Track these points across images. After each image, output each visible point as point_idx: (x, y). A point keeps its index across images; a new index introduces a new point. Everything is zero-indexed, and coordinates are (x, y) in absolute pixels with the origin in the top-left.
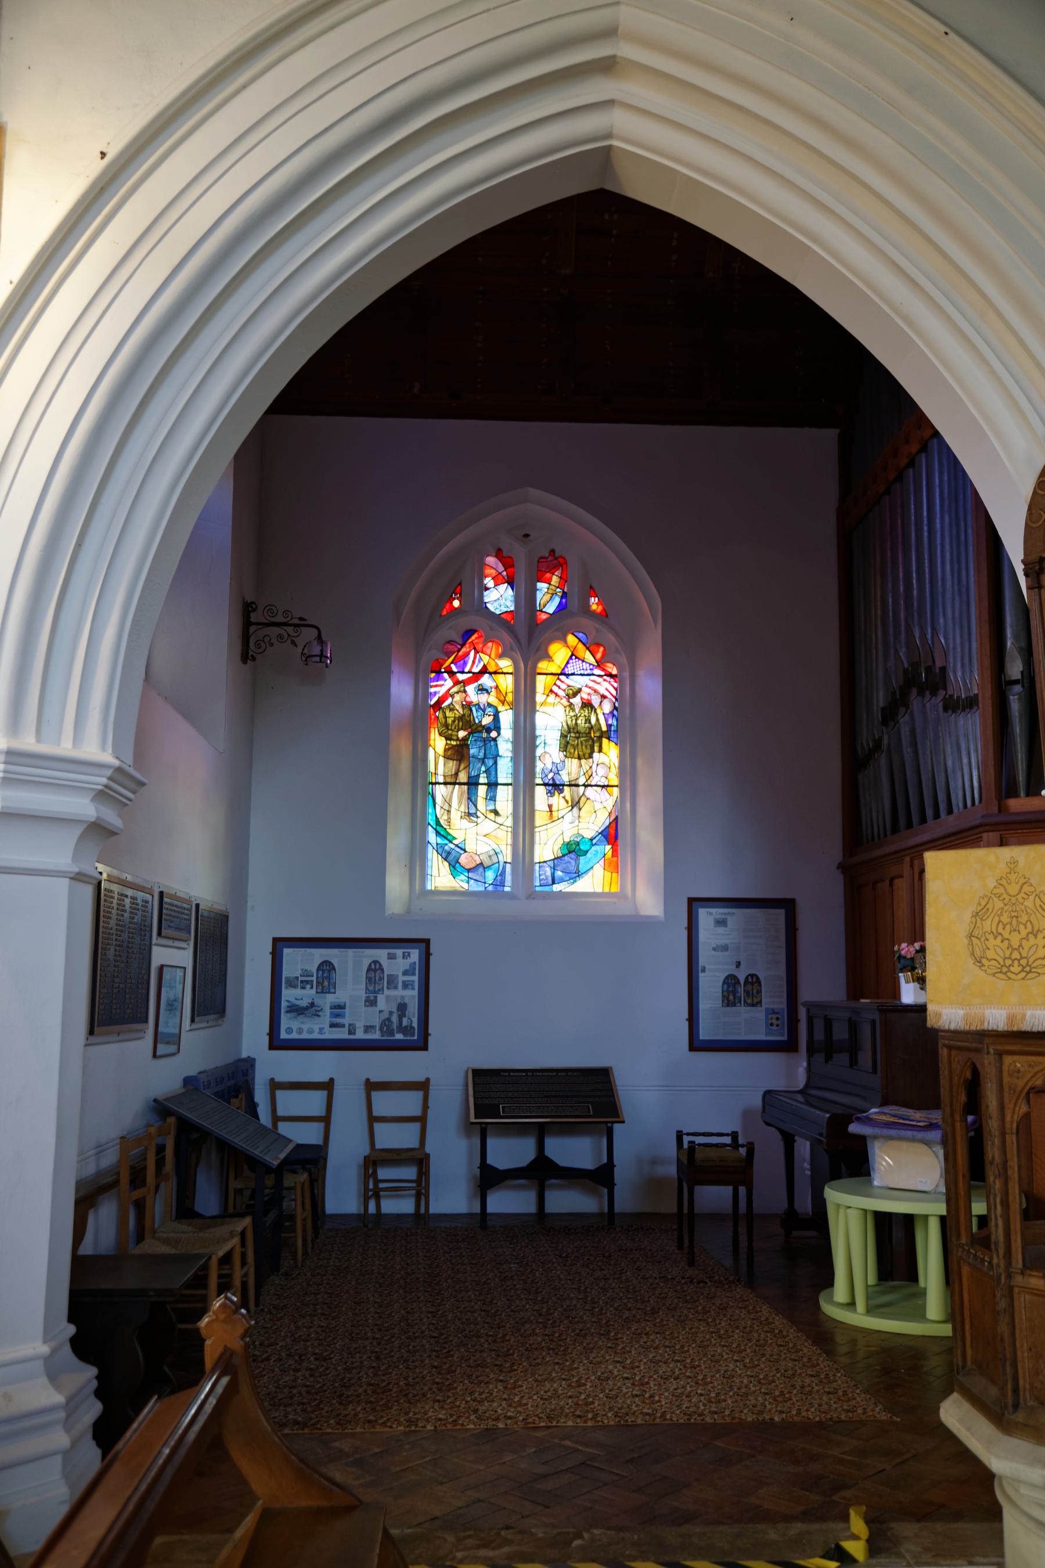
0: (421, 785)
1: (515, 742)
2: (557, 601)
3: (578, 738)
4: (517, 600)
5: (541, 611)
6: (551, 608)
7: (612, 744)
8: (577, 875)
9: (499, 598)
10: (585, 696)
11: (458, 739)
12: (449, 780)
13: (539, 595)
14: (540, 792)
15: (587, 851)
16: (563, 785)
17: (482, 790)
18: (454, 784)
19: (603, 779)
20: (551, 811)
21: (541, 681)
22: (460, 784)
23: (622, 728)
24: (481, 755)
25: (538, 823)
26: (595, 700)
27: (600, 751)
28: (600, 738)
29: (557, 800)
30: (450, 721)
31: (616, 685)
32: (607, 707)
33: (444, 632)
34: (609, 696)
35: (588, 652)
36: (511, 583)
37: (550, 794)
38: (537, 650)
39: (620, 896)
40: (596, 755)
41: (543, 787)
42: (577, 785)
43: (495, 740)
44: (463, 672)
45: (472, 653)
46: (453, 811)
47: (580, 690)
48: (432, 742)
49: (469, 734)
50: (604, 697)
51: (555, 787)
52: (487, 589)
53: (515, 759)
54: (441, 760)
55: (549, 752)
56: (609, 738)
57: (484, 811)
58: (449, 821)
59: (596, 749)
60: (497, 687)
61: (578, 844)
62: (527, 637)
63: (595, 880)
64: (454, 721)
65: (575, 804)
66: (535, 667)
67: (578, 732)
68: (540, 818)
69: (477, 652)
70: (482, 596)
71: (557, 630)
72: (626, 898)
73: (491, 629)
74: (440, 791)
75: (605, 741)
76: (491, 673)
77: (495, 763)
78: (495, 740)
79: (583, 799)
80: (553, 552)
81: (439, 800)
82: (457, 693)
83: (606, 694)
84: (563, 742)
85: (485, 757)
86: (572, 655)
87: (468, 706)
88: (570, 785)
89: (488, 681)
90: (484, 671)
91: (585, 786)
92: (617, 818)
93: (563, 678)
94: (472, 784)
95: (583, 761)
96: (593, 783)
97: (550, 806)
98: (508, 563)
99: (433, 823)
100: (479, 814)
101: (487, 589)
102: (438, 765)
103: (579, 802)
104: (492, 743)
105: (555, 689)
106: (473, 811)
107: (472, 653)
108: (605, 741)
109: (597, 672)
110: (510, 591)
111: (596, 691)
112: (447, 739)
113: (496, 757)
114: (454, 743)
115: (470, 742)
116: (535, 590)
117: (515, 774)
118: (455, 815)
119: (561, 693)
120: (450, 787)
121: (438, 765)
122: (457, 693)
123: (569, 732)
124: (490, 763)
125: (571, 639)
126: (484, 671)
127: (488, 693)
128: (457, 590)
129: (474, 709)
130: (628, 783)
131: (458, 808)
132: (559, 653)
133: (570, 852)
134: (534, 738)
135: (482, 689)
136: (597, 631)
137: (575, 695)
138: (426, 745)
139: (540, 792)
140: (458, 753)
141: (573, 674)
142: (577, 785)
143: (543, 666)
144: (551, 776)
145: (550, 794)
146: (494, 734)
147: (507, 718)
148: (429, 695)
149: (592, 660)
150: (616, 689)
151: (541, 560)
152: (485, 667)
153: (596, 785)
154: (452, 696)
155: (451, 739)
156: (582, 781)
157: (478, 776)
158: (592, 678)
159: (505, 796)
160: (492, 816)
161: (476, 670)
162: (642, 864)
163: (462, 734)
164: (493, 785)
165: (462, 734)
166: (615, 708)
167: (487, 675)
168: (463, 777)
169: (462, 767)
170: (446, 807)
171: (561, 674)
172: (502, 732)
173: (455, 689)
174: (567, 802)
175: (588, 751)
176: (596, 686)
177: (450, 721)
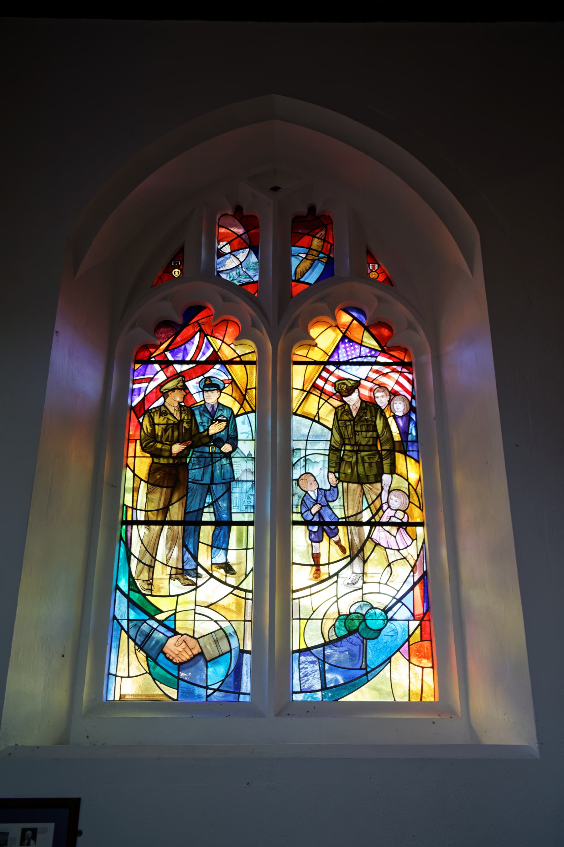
0: (107, 524)
1: (258, 458)
2: (319, 268)
3: (357, 452)
4: (262, 267)
5: (298, 281)
6: (312, 277)
7: (411, 462)
8: (363, 674)
9: (237, 264)
10: (365, 392)
11: (171, 455)
12: (152, 517)
13: (295, 262)
14: (299, 536)
15: (380, 630)
16: (337, 524)
17: (206, 533)
18: (162, 523)
19: (400, 514)
20: (317, 565)
21: (299, 376)
22: (172, 523)
23: (426, 433)
24: (207, 480)
25: (296, 583)
26: (382, 400)
27: (393, 471)
28: (391, 453)
29: (327, 549)
30: (159, 430)
31: (410, 376)
32: (400, 407)
33: (157, 306)
34: (403, 392)
35: (366, 334)
36: (255, 249)
37: (316, 538)
38: (292, 327)
39: (440, 707)
40: (386, 478)
41: (303, 528)
42: (360, 524)
43: (228, 456)
44: (183, 362)
45: (197, 336)
46: (158, 566)
47: (357, 385)
48: (130, 461)
49: (188, 449)
50: (394, 394)
51: (323, 527)
52: (221, 254)
53: (258, 484)
54: (143, 487)
55: (315, 469)
56: (405, 453)
57: (207, 565)
58: (150, 581)
59: (386, 468)
60: (233, 382)
61: (363, 618)
62: (278, 317)
63: (403, 680)
64: (165, 431)
65: (356, 554)
66: (288, 353)
67: (356, 444)
68: (301, 577)
69: (204, 335)
70: (211, 264)
71: (321, 300)
72: (451, 712)
73: (224, 299)
74: (138, 534)
75: (400, 458)
76: (224, 363)
77: (229, 491)
78: (228, 456)
79: (369, 546)
80: (312, 209)
81: (136, 548)
82: (173, 390)
83: (397, 388)
84: (334, 457)
85: (212, 482)
86: (344, 337)
87: (187, 408)
88: (346, 524)
89: (219, 372)
90: (215, 359)
91: (372, 524)
92: (425, 574)
93: (332, 368)
94: (191, 523)
95: (367, 487)
96: (384, 520)
97: (316, 557)
98: (250, 223)
99: (123, 584)
100: (200, 570)
101: (221, 254)
102: (137, 496)
103: (362, 549)
104: (224, 461)
105: (320, 383)
106: (190, 565)
107: (197, 336)
108: (400, 458)
109: (381, 359)
110: (253, 258)
111: (381, 386)
112: (153, 456)
113: (229, 482)
114: (163, 461)
115: (188, 465)
116: (288, 256)
117: (258, 508)
118: (161, 573)
119: (329, 388)
120: (155, 528)
121: (137, 496)
122: (173, 390)
123: (344, 444)
124: (219, 490)
125: (345, 318)
126: (215, 359)
127: (220, 390)
128: (178, 258)
129: (197, 412)
130: (441, 516)
131: (167, 552)
132: (325, 338)
133: (350, 633)
134: (289, 451)
135: (209, 385)
136: (380, 299)
137: (350, 391)
138: (119, 464)
139: (299, 536)
140: (168, 476)
141: (347, 363)
142: (360, 524)
143: (300, 353)
144: (315, 510)
145: (316, 538)
146: (227, 448)
147: (245, 427)
148: (126, 392)
149: (373, 344)
150: (411, 382)
151: (297, 220)
152: (215, 352)
153: (388, 524)
154: (165, 395)
155: (159, 456)
156: (366, 516)
157: (200, 511)
158: (376, 367)
159: (240, 550)
160: (220, 573)
161: (202, 358)
162: (479, 649)
163: (177, 448)
164: (223, 525)
165: (177, 448)
166: (412, 409)
167: (218, 366)
168: (176, 512)
169: (175, 498)
170: (147, 559)
171: (329, 363)
172: (240, 444)
173: (170, 385)
174: (343, 550)
175: (374, 471)
176: (383, 380)
177: (159, 430)
